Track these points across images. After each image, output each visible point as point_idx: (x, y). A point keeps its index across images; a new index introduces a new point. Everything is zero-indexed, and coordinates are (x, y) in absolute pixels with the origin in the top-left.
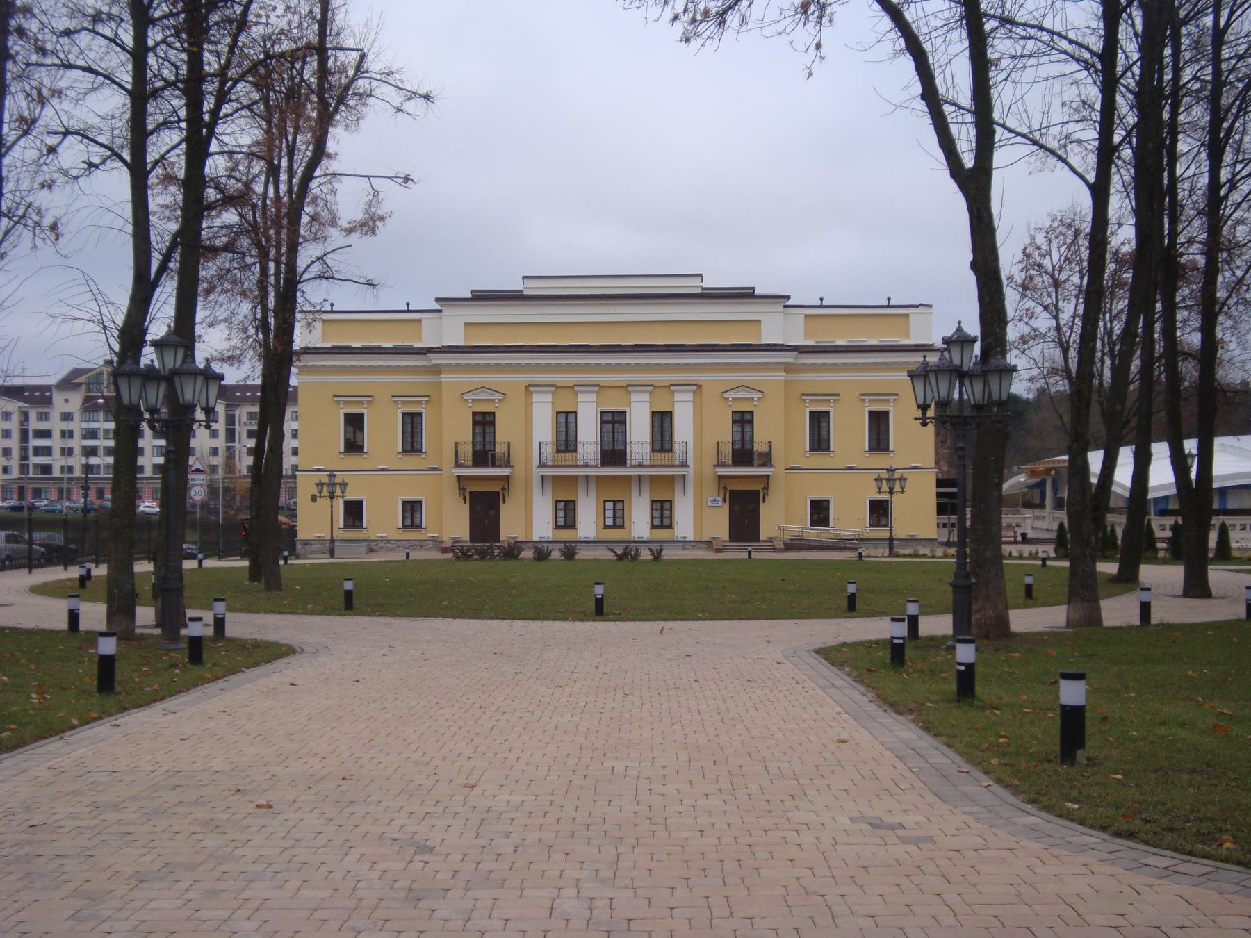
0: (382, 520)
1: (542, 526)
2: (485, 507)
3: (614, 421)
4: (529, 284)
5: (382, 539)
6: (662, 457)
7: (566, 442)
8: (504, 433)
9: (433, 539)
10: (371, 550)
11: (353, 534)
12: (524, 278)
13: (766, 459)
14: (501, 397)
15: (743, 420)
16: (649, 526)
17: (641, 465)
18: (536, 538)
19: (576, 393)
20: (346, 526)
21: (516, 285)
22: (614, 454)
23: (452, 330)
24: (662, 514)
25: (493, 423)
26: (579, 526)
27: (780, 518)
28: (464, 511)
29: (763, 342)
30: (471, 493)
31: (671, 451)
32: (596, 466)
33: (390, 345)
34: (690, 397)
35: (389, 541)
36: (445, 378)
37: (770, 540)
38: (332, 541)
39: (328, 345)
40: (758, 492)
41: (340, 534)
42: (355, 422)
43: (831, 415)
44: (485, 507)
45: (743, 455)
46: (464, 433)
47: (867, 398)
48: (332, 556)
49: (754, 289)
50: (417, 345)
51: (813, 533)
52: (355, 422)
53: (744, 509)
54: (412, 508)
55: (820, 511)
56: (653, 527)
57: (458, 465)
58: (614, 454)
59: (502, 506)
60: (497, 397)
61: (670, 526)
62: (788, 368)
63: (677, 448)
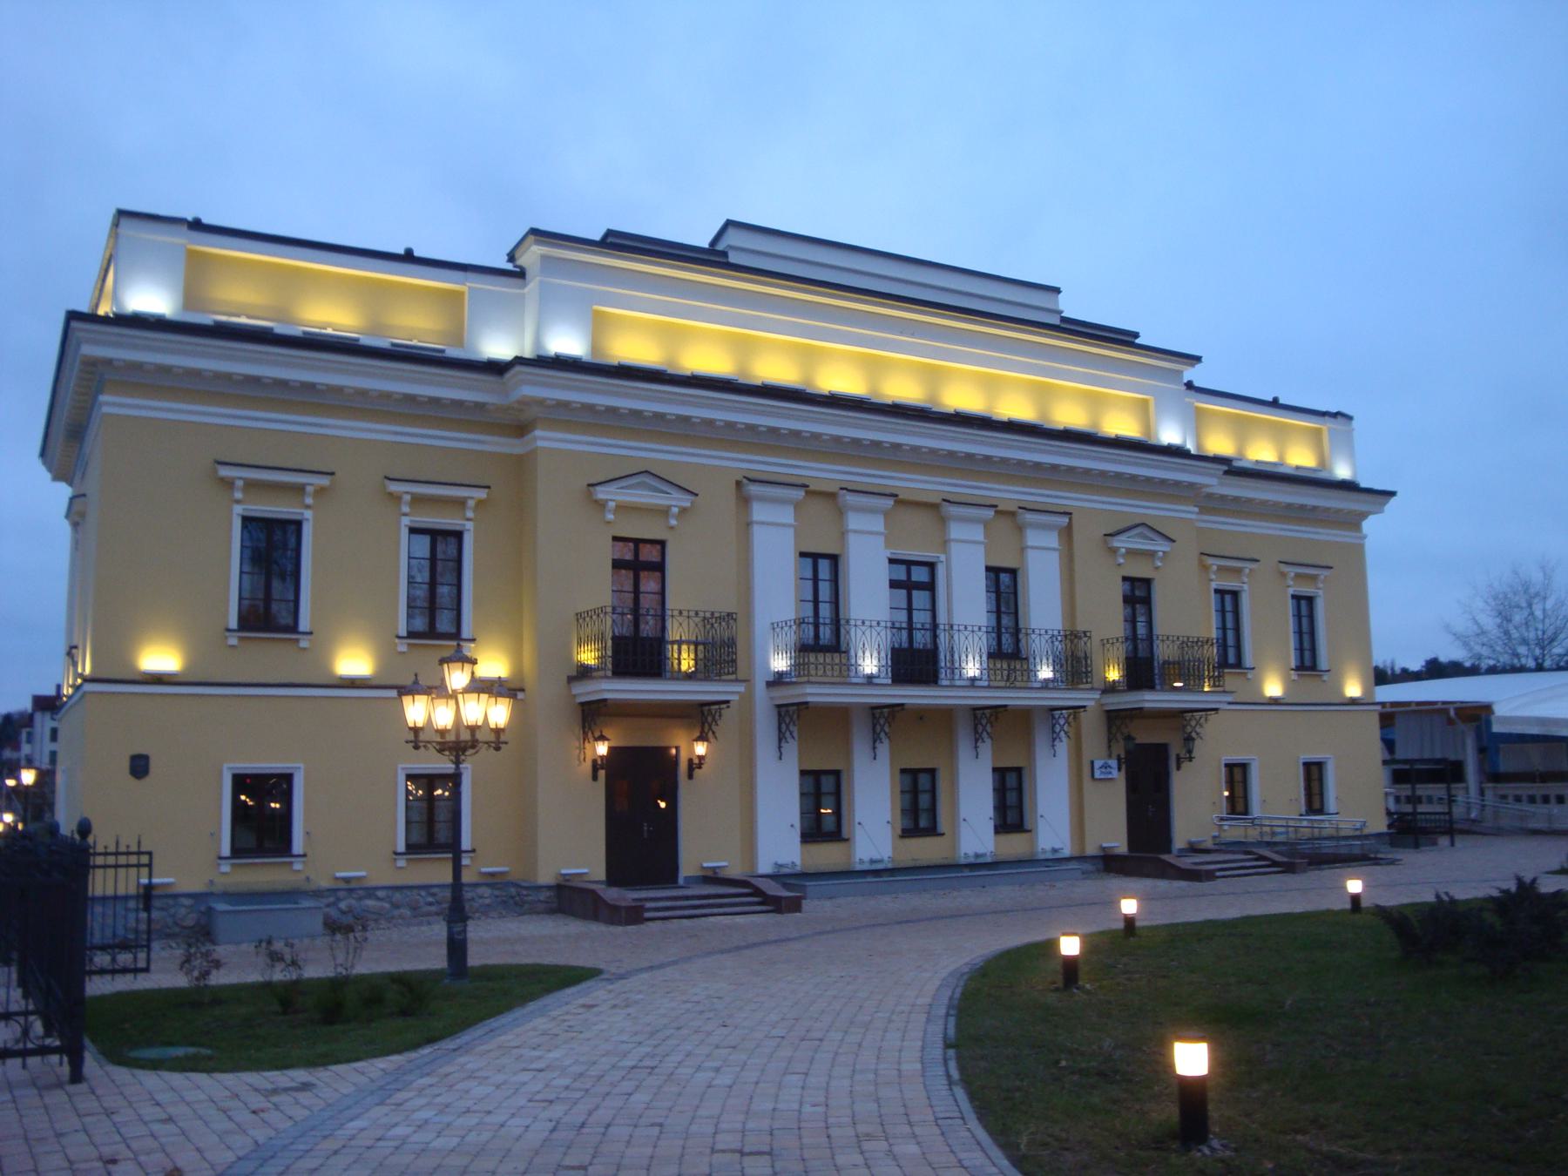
3: (915, 581)
20: (237, 852)
22: (916, 661)
25: (659, 567)
43: (307, 531)
60: (677, 500)
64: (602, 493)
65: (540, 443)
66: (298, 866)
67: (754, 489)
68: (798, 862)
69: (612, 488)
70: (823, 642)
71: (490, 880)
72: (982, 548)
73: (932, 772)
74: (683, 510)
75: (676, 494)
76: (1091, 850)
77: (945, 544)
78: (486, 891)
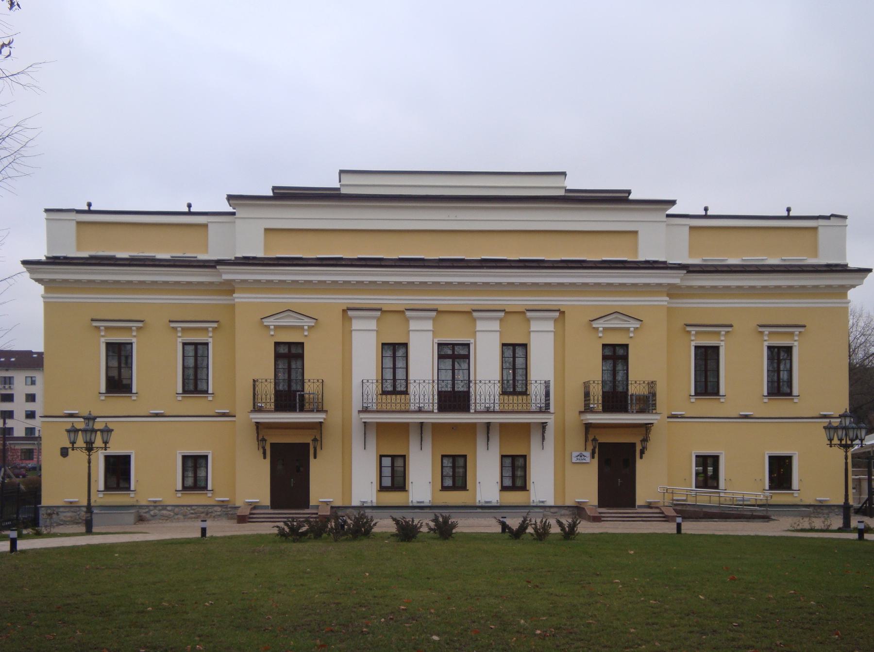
0: (156, 479)
1: (364, 489)
2: (290, 467)
3: (454, 355)
4: (348, 180)
5: (156, 505)
8: (315, 369)
9: (223, 505)
10: (141, 519)
11: (117, 498)
12: (342, 172)
13: (647, 403)
14: (312, 323)
15: (616, 356)
16: (498, 487)
17: (488, 411)
18: (355, 502)
19: (407, 320)
21: (332, 182)
22: (454, 399)
23: (249, 238)
24: (516, 472)
25: (301, 356)
26: (532, 487)
27: (660, 478)
28: (264, 467)
29: (641, 258)
30: (271, 444)
31: (525, 393)
32: (432, 412)
33: (166, 256)
34: (550, 326)
35: (164, 507)
36: (240, 298)
37: (649, 506)
38: (89, 508)
39: (85, 254)
40: (633, 445)
41: (100, 498)
42: (119, 353)
44: (290, 467)
45: (616, 399)
46: (263, 367)
47: (766, 331)
48: (89, 531)
49: (629, 192)
50: (202, 257)
51: (705, 498)
52: (119, 353)
53: (617, 467)
54: (194, 464)
55: (708, 470)
56: (504, 488)
57: (257, 409)
58: (454, 399)
59: (312, 461)
60: (307, 323)
61: (524, 488)
62: (673, 292)
63: (536, 390)
64: (266, 322)
65: (236, 300)
66: (132, 495)
67: (350, 313)
68: (374, 501)
69: (272, 319)
70: (395, 387)
71: (222, 504)
72: (552, 335)
73: (465, 457)
74: (310, 327)
75: (306, 320)
76: (569, 503)
77: (474, 333)
78: (219, 509)
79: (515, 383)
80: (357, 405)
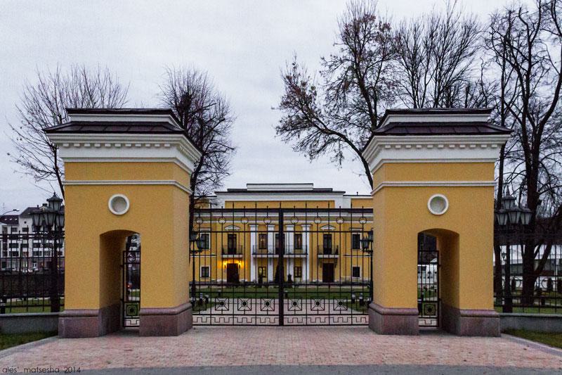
6: (297, 251)
7: (263, 246)
15: (328, 238)
21: (244, 187)
22: (280, 249)
24: (298, 272)
45: (327, 250)
51: (354, 279)
53: (328, 270)
63: (304, 248)
79: (298, 245)
80: (252, 253)
